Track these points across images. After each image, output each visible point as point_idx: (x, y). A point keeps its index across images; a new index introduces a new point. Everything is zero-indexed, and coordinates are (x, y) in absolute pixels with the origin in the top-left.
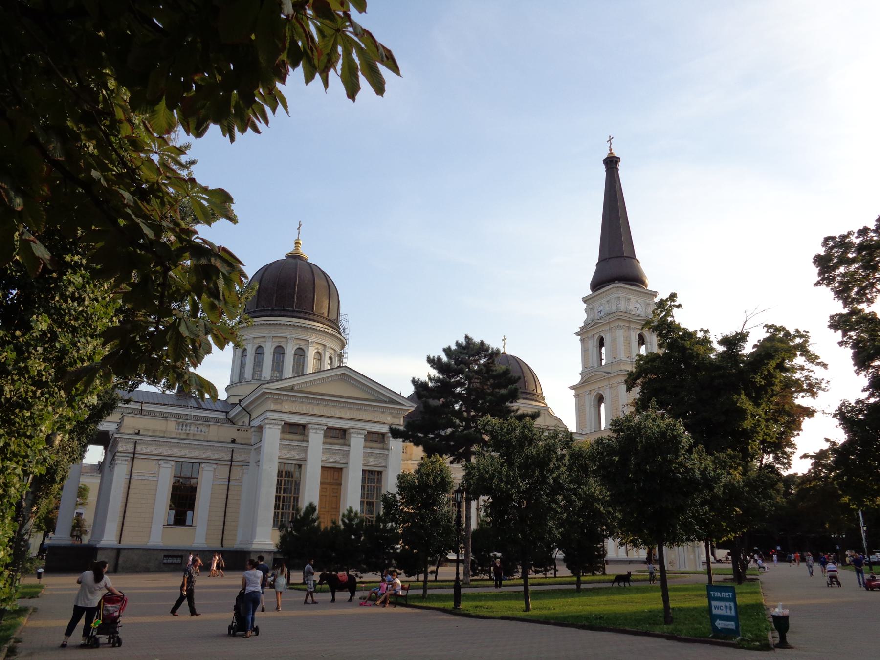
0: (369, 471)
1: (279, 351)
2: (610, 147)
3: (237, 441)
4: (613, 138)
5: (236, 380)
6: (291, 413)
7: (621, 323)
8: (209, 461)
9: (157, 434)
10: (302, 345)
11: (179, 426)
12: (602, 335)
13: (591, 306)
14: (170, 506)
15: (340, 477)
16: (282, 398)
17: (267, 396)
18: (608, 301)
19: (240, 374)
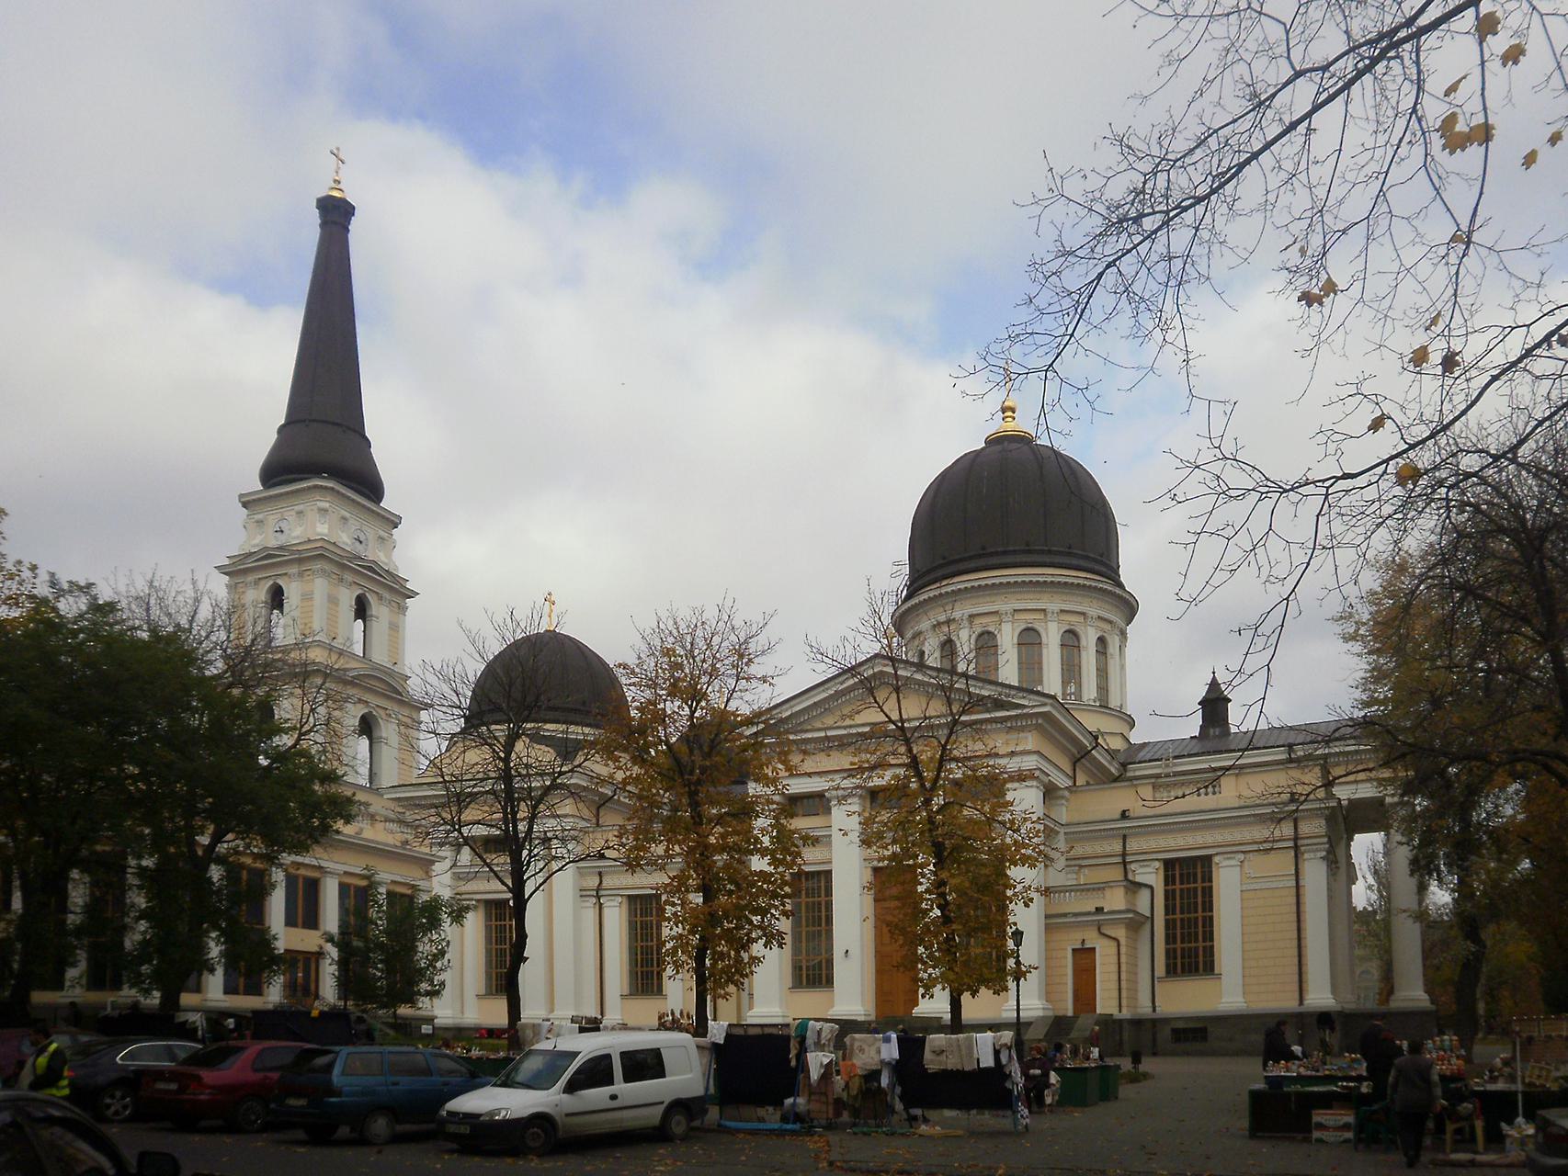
7: (327, 567)
12: (280, 582)
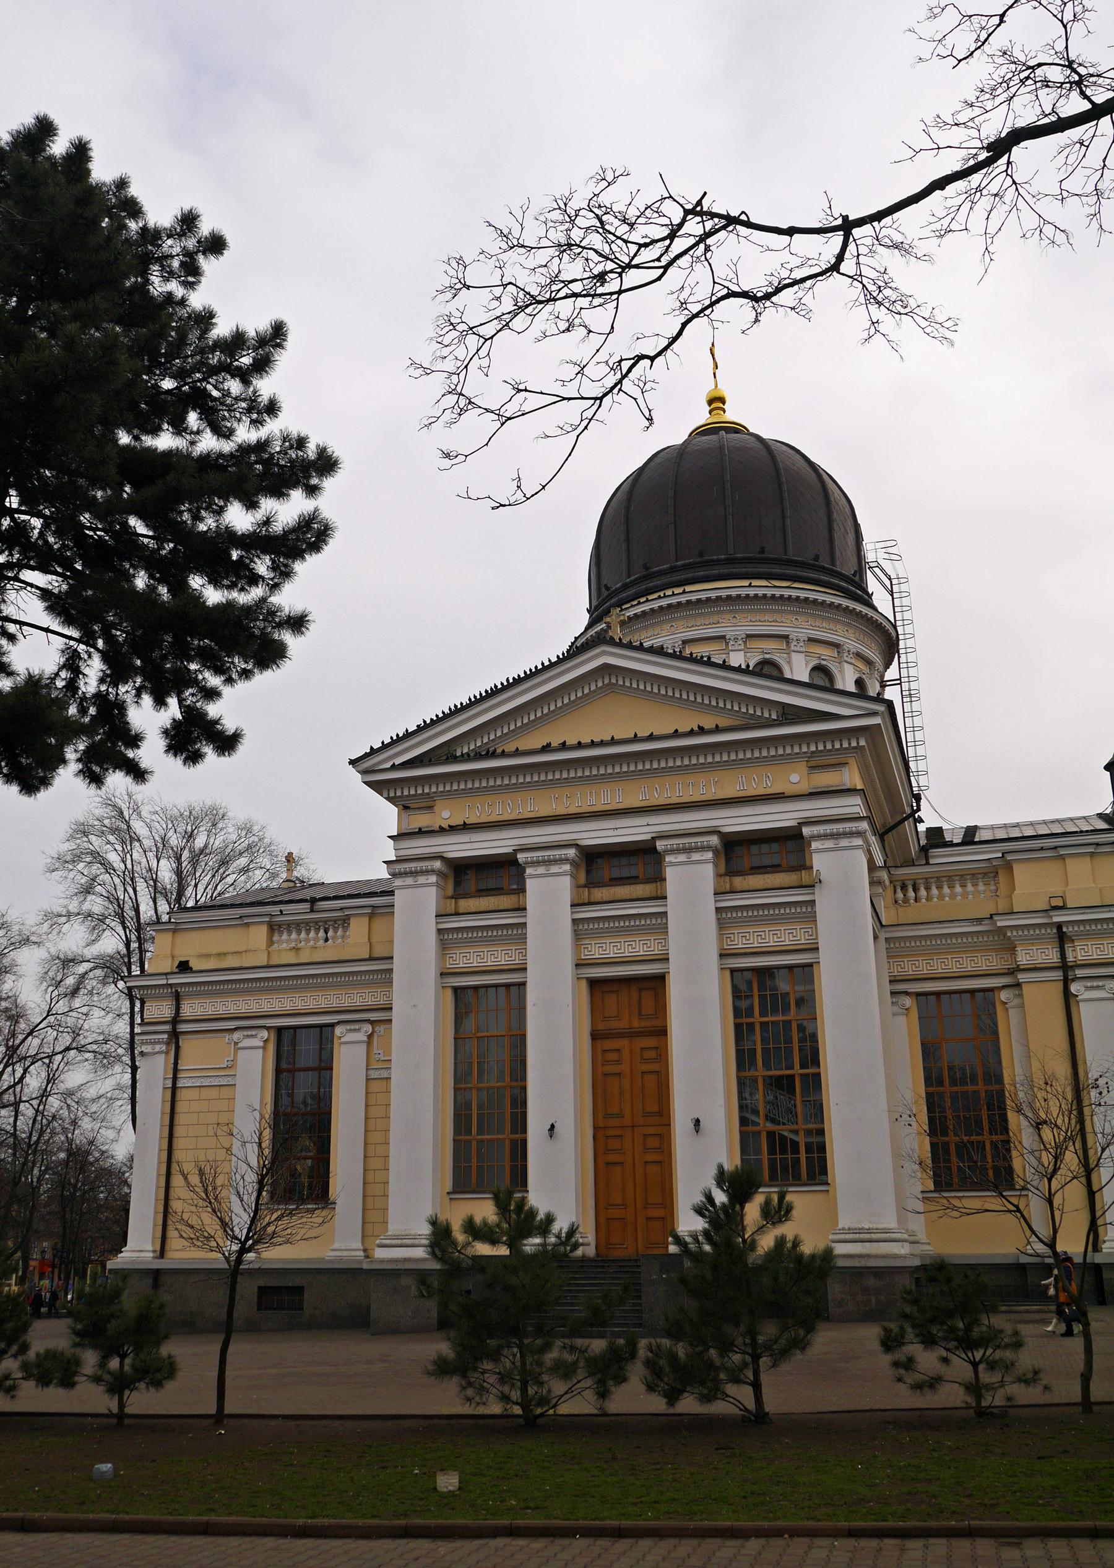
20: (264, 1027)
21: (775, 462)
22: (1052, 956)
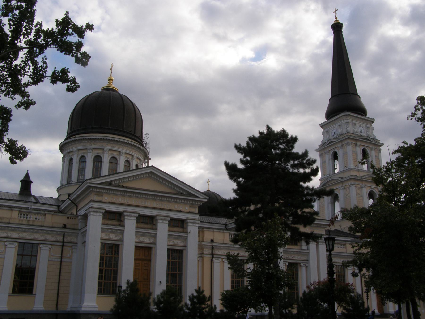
0: (172, 250)
1: (98, 160)
2: (336, 16)
3: (68, 226)
4: (337, 10)
5: (65, 182)
6: (110, 203)
7: (350, 141)
8: (46, 242)
9: (4, 220)
10: (116, 154)
11: (21, 214)
12: (336, 150)
13: (327, 130)
14: (15, 278)
15: (150, 254)
16: (103, 191)
17: (91, 189)
18: (340, 126)
19: (68, 178)
20: (17, 242)
21: (123, 103)
22: (209, 252)
